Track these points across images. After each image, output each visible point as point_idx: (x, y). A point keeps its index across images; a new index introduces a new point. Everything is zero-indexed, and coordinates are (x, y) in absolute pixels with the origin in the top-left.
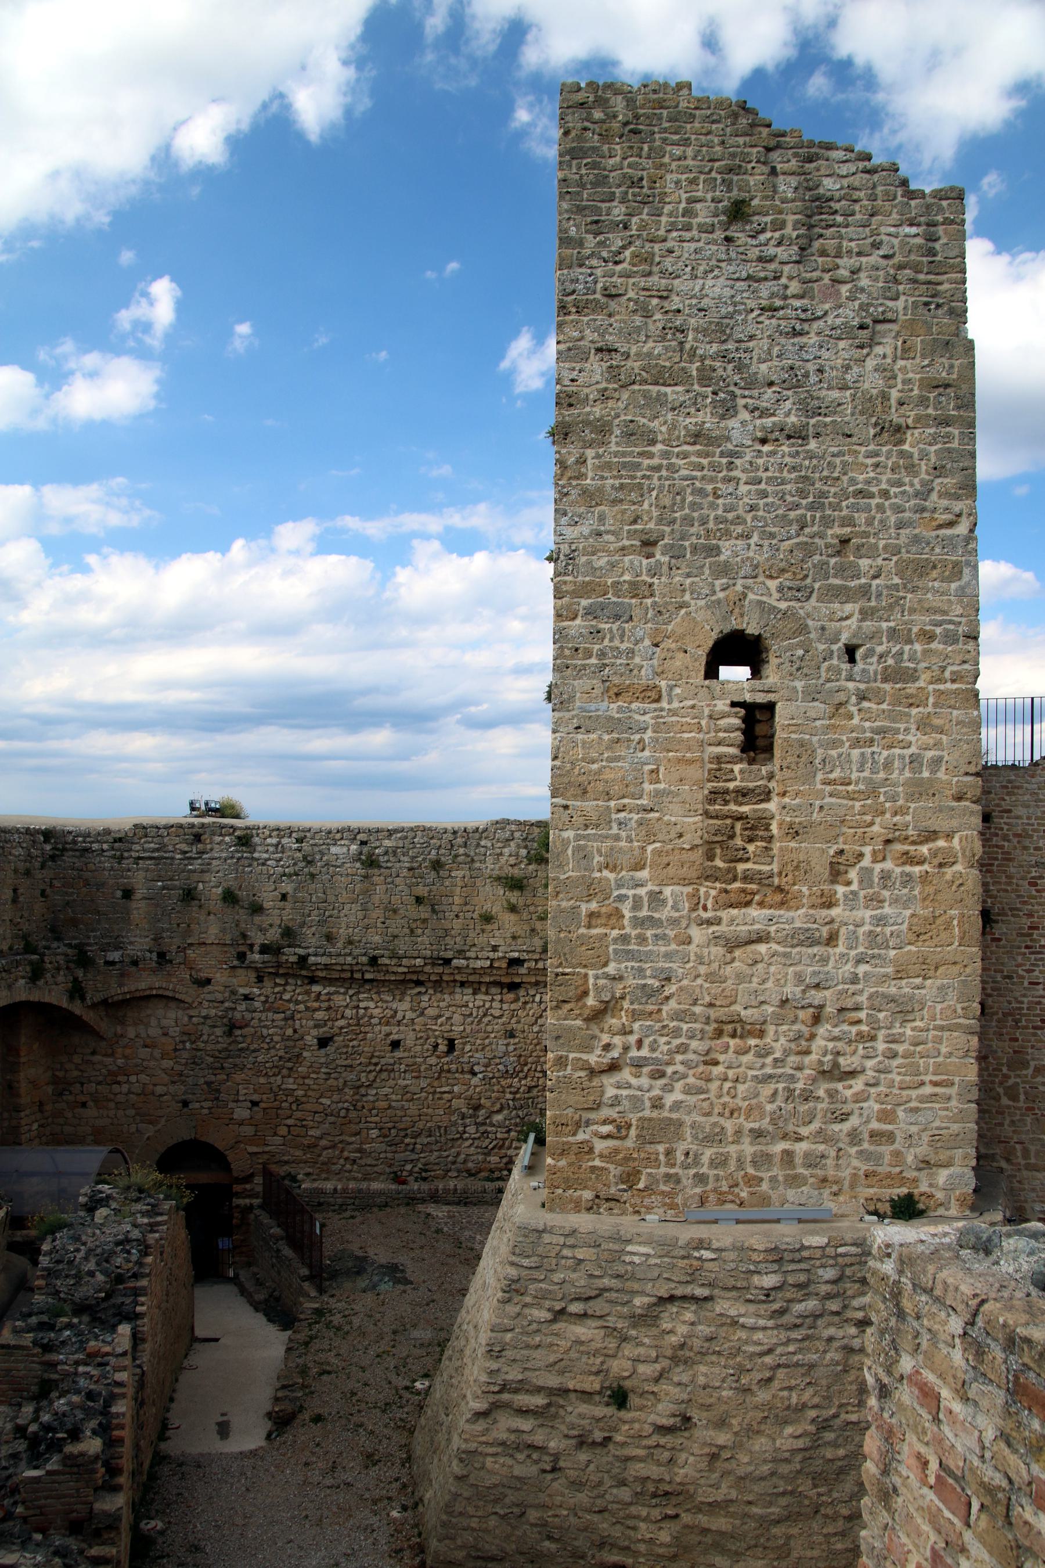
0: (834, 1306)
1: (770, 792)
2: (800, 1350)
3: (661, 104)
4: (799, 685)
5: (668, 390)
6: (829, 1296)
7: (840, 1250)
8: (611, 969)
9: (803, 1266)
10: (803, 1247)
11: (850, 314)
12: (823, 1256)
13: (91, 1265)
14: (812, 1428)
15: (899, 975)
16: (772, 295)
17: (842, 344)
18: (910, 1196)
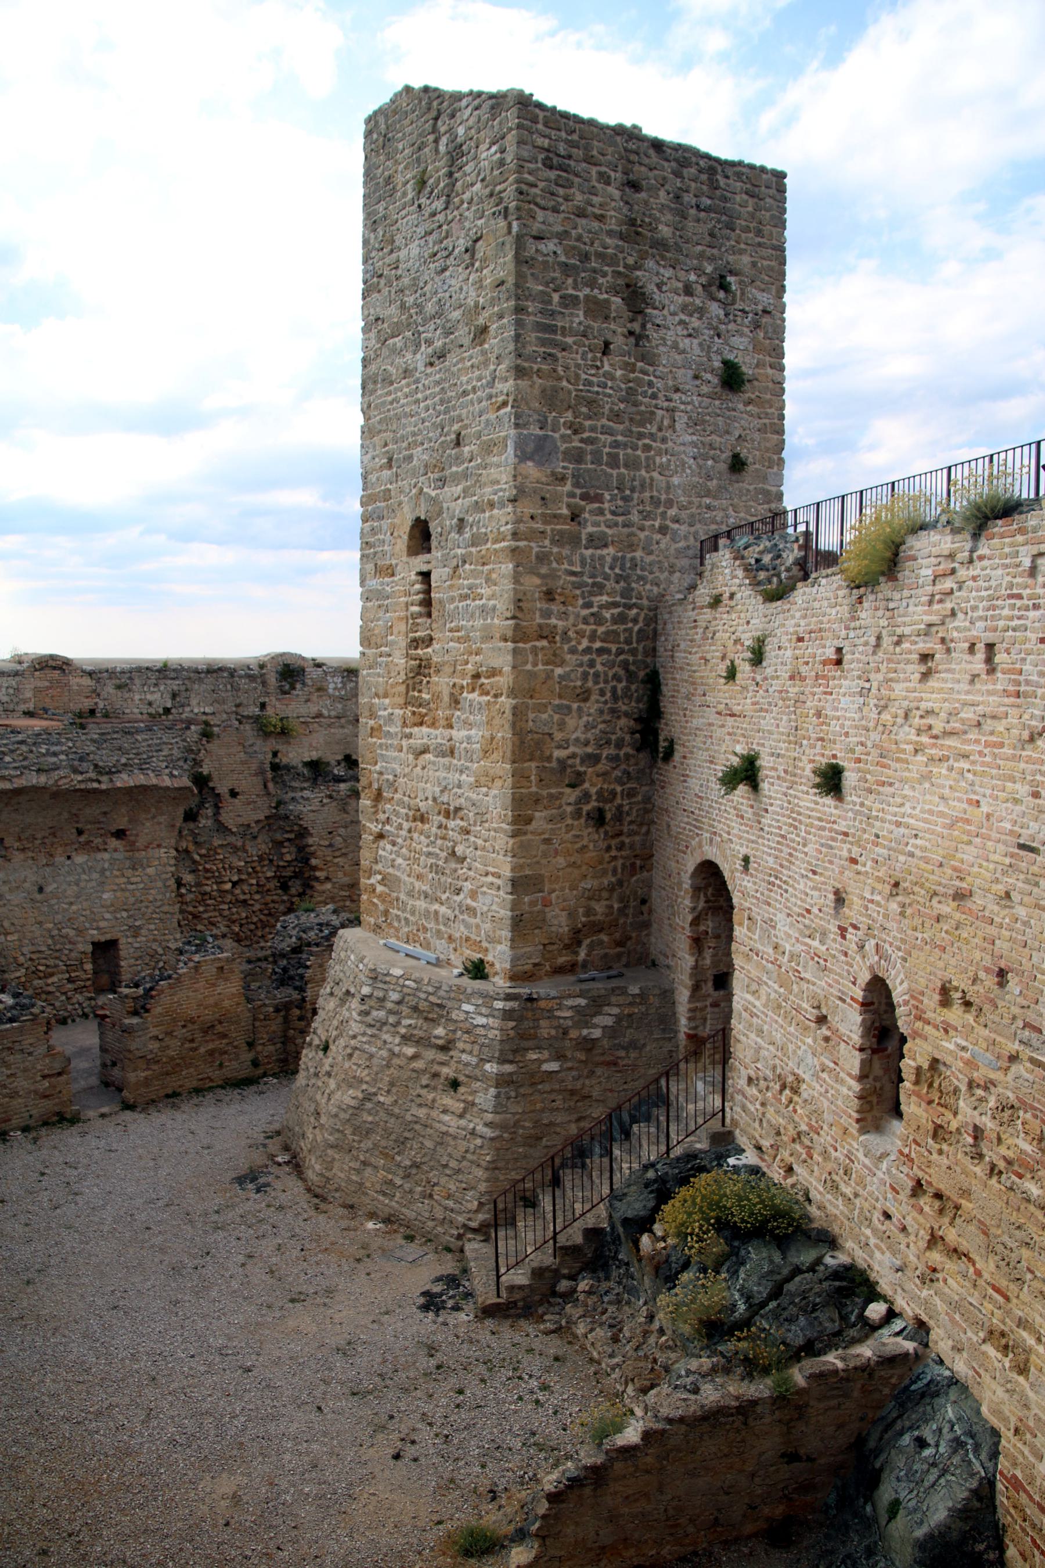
0: (392, 1019)
1: (431, 639)
2: (369, 1043)
3: (395, 112)
4: (439, 554)
5: (396, 340)
6: (391, 1012)
7: (407, 983)
8: (377, 768)
9: (385, 987)
10: (388, 974)
11: (462, 243)
12: (396, 984)
13: (294, 932)
14: (360, 1095)
15: (478, 785)
16: (435, 243)
17: (460, 269)
18: (482, 961)
